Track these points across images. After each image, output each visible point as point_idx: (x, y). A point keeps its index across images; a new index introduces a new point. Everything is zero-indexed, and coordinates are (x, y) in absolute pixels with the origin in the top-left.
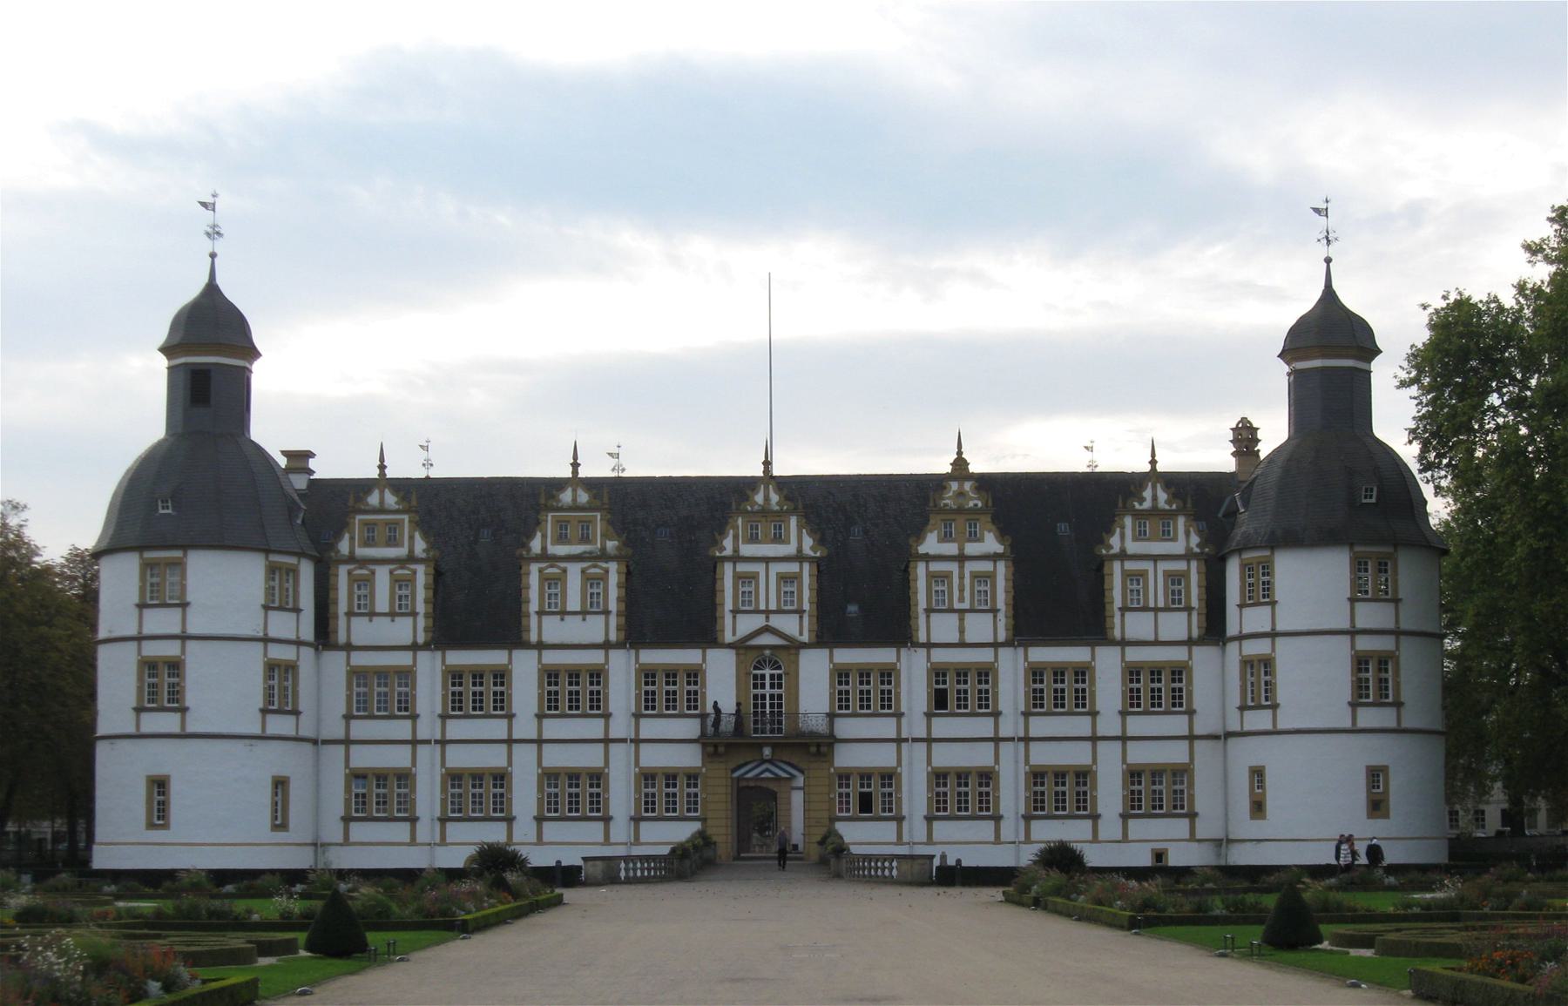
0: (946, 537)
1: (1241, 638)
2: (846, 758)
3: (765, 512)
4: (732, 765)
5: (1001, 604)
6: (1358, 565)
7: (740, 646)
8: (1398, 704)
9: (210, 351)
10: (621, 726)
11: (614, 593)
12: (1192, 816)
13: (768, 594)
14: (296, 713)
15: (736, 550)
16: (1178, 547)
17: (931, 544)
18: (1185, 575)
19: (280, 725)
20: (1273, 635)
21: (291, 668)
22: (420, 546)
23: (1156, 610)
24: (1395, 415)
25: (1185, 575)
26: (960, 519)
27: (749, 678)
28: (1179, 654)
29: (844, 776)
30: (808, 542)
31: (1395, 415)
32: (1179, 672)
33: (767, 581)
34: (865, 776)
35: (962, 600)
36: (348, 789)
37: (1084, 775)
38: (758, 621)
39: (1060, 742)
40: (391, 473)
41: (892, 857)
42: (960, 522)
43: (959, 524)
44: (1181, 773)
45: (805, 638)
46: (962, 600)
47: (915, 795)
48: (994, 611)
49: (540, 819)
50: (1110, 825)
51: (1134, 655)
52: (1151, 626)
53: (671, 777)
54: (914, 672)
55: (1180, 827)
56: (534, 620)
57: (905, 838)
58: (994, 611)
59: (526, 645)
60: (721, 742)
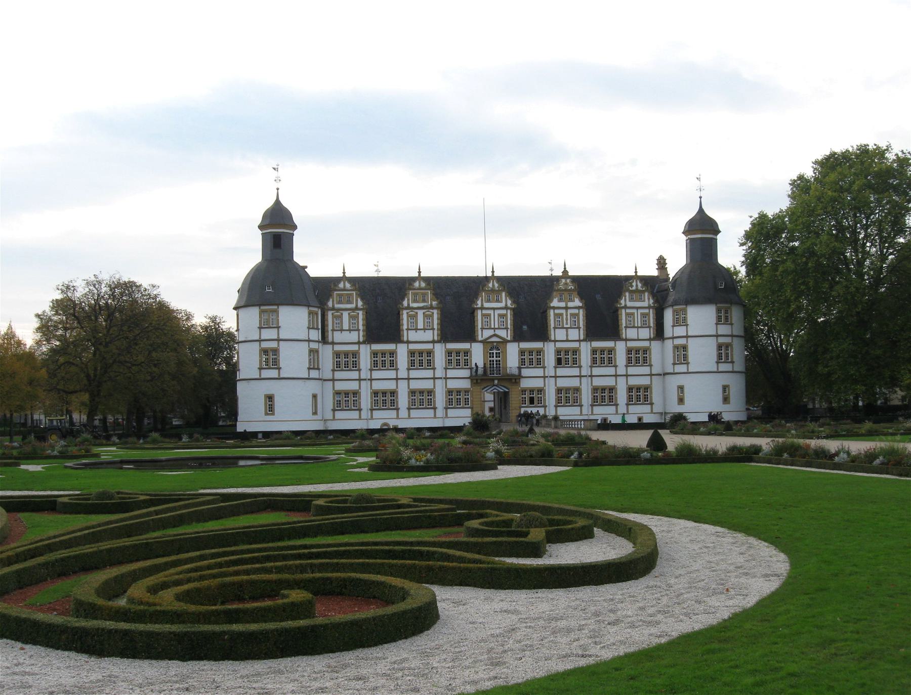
0: (560, 300)
1: (673, 338)
2: (525, 384)
3: (493, 290)
5: (581, 325)
6: (719, 311)
7: (484, 342)
8: (732, 362)
9: (278, 227)
10: (439, 373)
11: (436, 322)
12: (652, 404)
13: (495, 322)
14: (318, 369)
15: (482, 305)
16: (645, 304)
17: (555, 303)
18: (648, 314)
19: (314, 374)
20: (687, 337)
21: (317, 351)
22: (360, 303)
23: (638, 327)
24: (731, 255)
25: (648, 314)
26: (566, 293)
27: (488, 354)
28: (646, 344)
29: (524, 391)
30: (509, 302)
31: (731, 255)
32: (646, 350)
33: (494, 316)
34: (532, 391)
35: (567, 323)
36: (334, 399)
37: (612, 389)
38: (491, 332)
39: (603, 377)
40: (347, 275)
41: (581, 420)
42: (565, 294)
43: (566, 295)
44: (647, 388)
45: (509, 338)
46: (567, 323)
47: (551, 397)
48: (579, 328)
49: (409, 409)
51: (631, 344)
52: (636, 333)
53: (459, 392)
54: (549, 351)
55: (647, 408)
56: (405, 332)
58: (579, 328)
59: (403, 342)
60: (480, 379)
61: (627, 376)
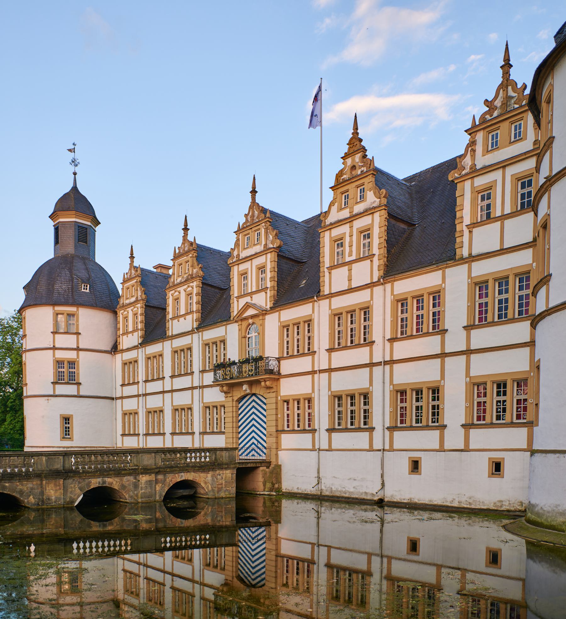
2: (289, 388)
4: (235, 398)
27: (244, 338)
50: (454, 437)
55: (517, 437)
57: (317, 447)
61: (468, 352)
